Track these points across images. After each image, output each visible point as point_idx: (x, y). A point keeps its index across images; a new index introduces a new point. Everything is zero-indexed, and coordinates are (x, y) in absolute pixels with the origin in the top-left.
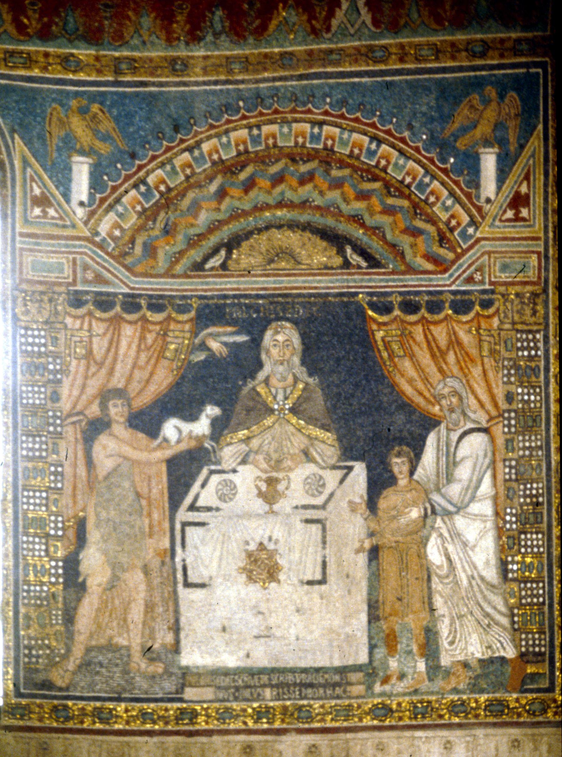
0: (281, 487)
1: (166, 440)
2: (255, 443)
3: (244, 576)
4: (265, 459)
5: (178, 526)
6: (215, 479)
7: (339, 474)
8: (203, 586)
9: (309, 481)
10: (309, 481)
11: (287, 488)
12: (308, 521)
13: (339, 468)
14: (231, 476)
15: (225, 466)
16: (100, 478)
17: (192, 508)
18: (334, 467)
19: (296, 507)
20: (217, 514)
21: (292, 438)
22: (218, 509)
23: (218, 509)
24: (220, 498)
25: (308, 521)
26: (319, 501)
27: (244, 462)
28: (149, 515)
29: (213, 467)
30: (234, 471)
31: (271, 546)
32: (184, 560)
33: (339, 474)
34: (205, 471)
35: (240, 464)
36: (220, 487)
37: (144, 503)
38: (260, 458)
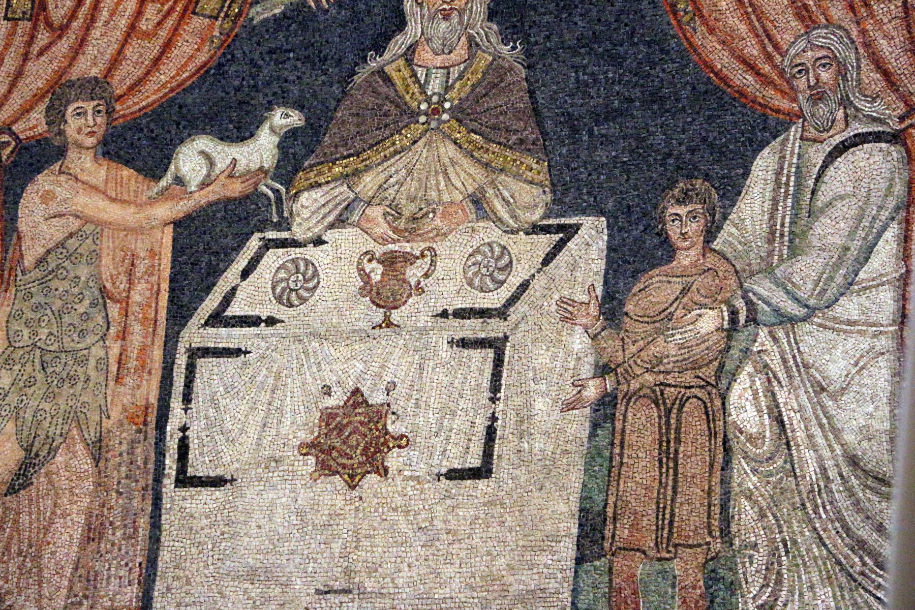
0: (413, 273)
1: (179, 180)
2: (368, 183)
3: (312, 460)
4: (385, 214)
5: (181, 360)
6: (273, 259)
7: (545, 242)
8: (217, 482)
9: (479, 258)
10: (479, 258)
11: (426, 275)
12: (464, 343)
13: (546, 229)
14: (310, 252)
15: (299, 232)
16: (29, 260)
17: (217, 319)
18: (536, 229)
19: (444, 314)
20: (270, 330)
21: (450, 170)
22: (271, 321)
23: (271, 321)
24: (279, 299)
25: (464, 343)
26: (494, 300)
27: (340, 222)
28: (123, 335)
29: (271, 235)
30: (318, 242)
31: (377, 398)
32: (184, 429)
33: (545, 242)
34: (254, 243)
35: (331, 226)
36: (282, 274)
37: (114, 310)
38: (376, 212)
